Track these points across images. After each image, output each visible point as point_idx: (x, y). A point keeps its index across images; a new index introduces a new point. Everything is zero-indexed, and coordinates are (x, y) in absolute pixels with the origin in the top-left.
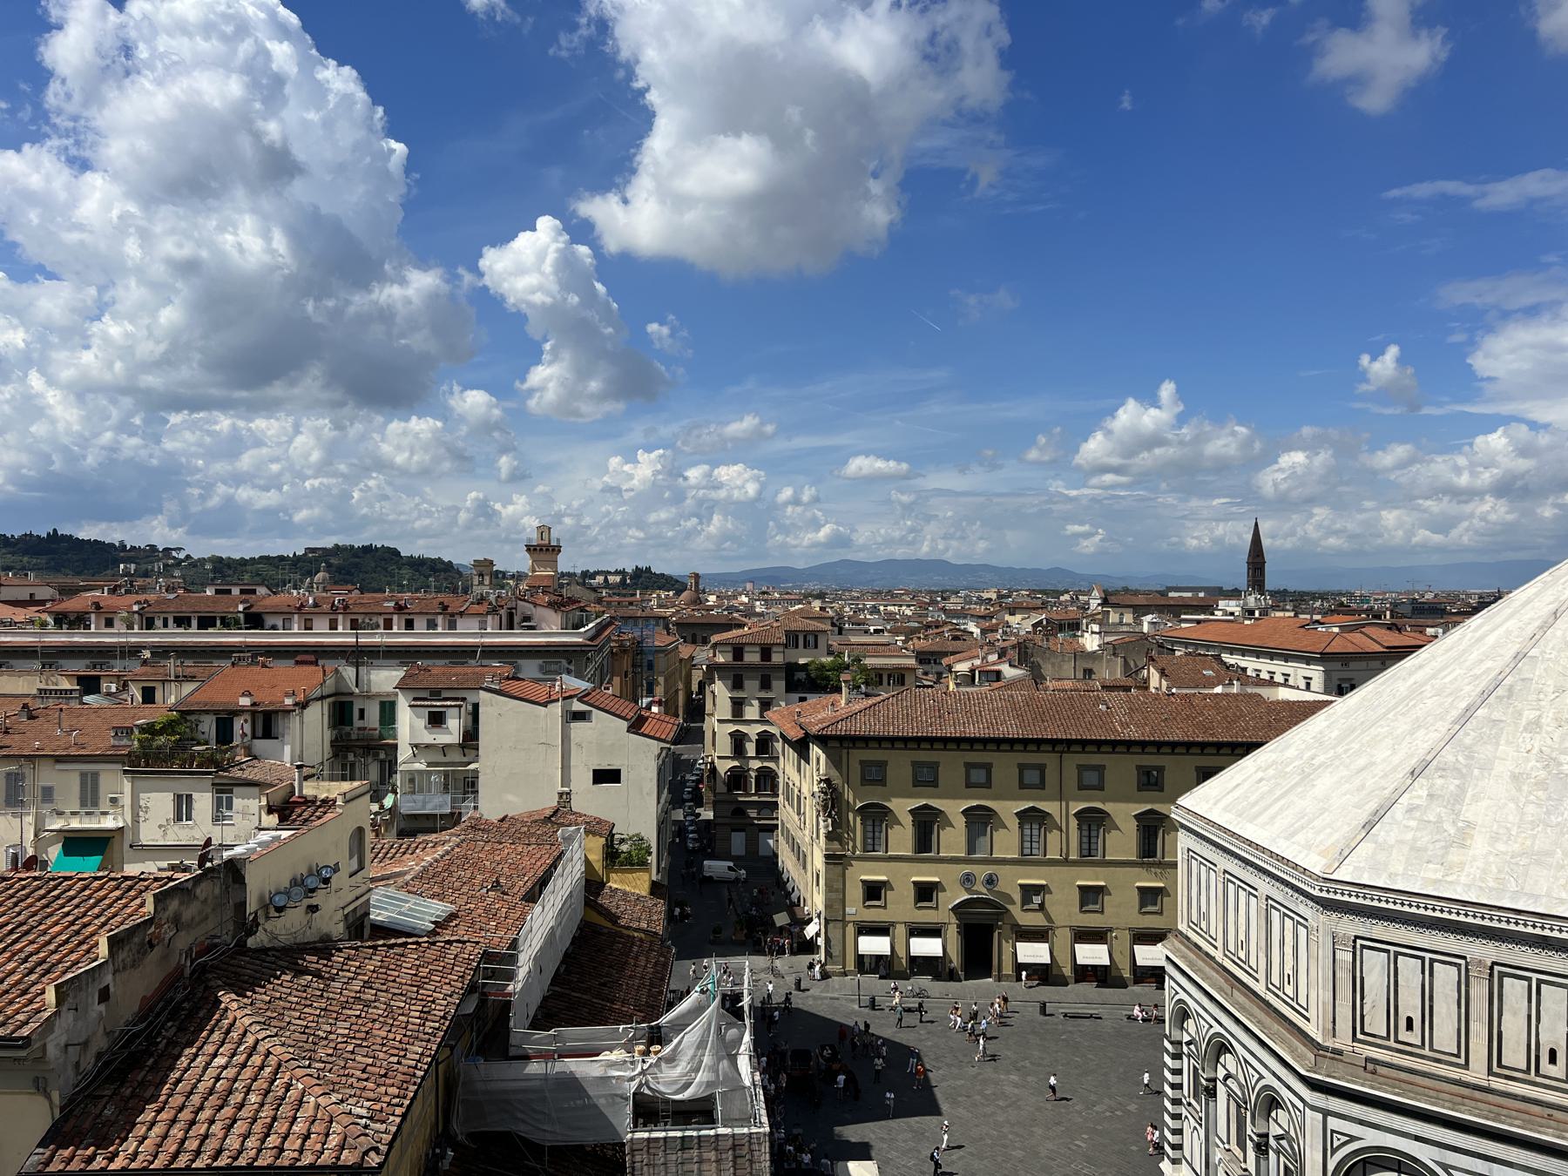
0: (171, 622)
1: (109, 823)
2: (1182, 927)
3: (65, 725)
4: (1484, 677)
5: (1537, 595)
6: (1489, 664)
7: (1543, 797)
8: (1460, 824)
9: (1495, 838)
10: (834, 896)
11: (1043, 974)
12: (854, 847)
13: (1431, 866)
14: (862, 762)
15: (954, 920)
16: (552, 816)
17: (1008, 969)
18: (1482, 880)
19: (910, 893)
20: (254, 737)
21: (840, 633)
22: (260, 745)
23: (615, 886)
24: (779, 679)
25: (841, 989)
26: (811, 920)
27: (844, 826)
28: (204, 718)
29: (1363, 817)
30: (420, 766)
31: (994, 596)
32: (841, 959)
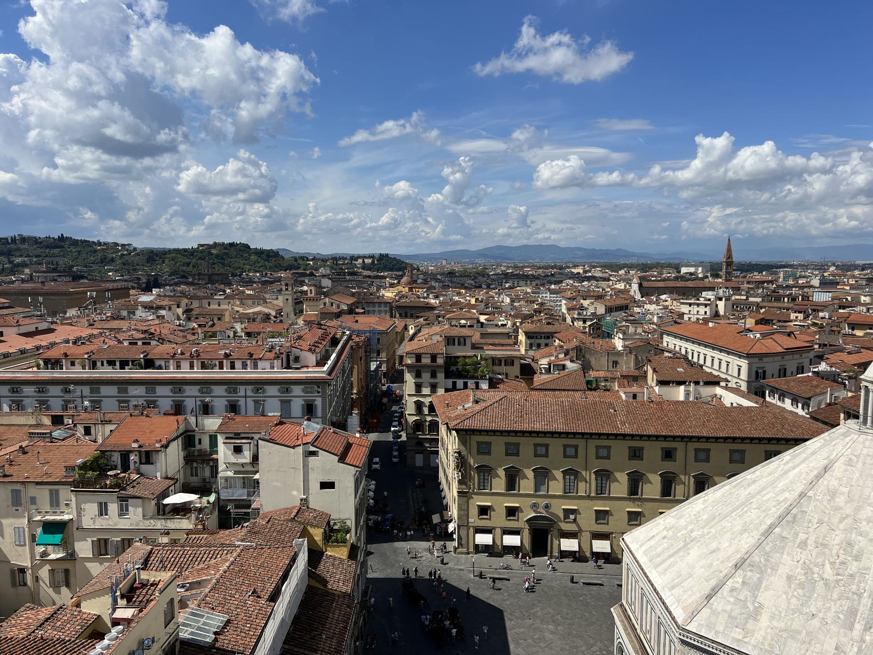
0: (105, 363)
1: (66, 517)
2: (624, 602)
3: (41, 458)
4: (783, 504)
5: (820, 448)
6: (786, 495)
7: (801, 594)
8: (756, 605)
9: (772, 618)
10: (462, 513)
11: (576, 557)
12: (474, 488)
13: (738, 630)
14: (478, 443)
15: (527, 527)
16: (295, 516)
18: (763, 644)
19: (504, 512)
20: (141, 463)
21: (482, 327)
22: (145, 468)
23: (330, 554)
25: (465, 563)
26: (451, 521)
27: (468, 477)
28: (113, 453)
29: (707, 591)
30: (230, 474)
31: (581, 271)
32: (466, 546)
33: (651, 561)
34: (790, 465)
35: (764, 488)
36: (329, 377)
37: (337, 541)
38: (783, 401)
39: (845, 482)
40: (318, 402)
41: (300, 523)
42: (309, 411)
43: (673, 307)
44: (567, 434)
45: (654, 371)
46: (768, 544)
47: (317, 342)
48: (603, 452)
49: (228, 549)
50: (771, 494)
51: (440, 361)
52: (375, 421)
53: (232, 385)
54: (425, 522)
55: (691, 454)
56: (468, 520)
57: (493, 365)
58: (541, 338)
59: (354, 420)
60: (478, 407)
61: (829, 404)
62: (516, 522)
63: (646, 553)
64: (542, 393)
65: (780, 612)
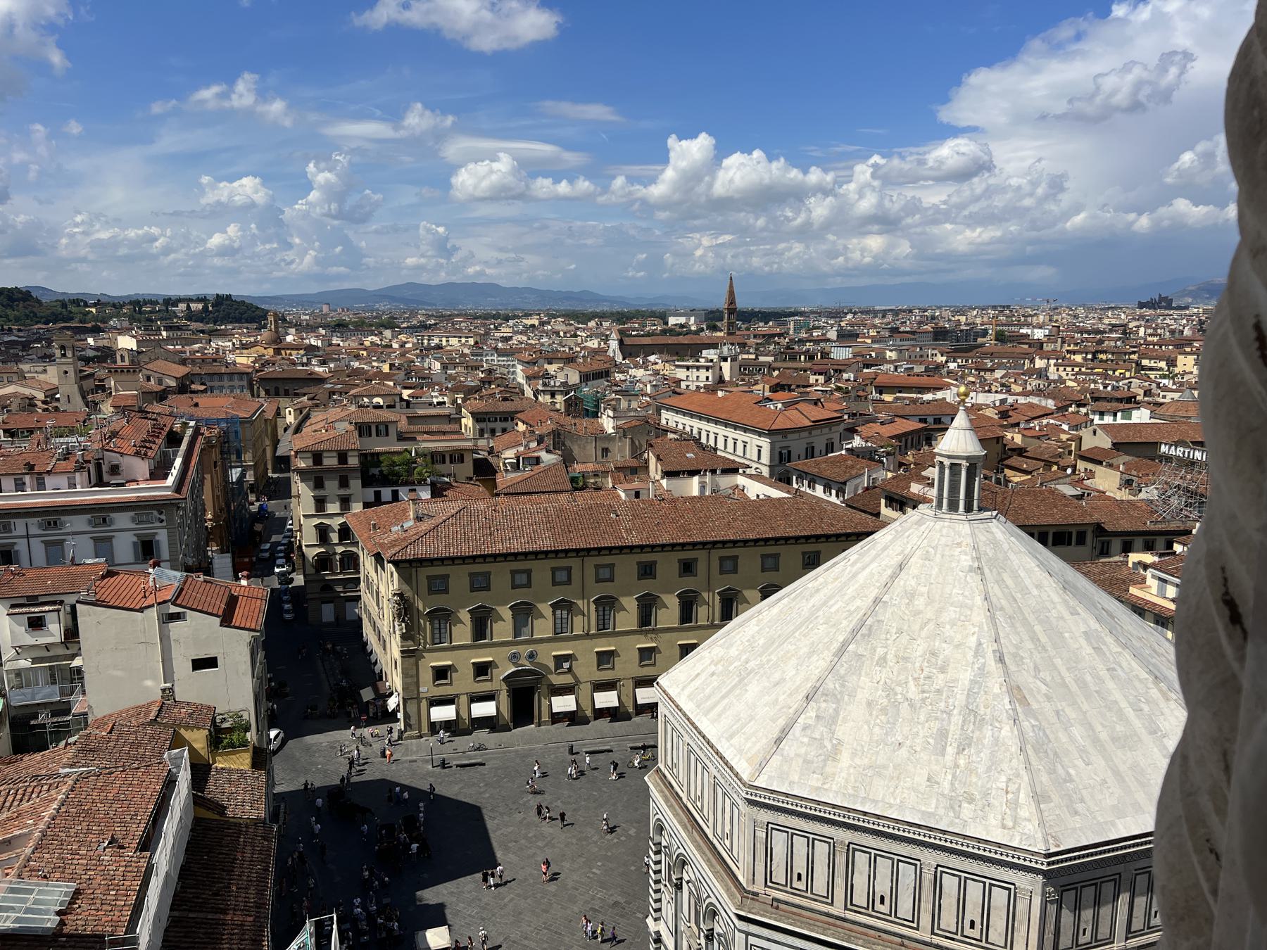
2: (661, 766)
5: (892, 541)
6: (858, 603)
8: (834, 742)
9: (854, 755)
10: (409, 680)
11: (572, 718)
12: (425, 643)
13: (815, 776)
14: (428, 577)
15: (505, 687)
16: (157, 717)
17: (546, 717)
18: (846, 788)
19: (470, 671)
21: (408, 407)
23: (221, 766)
24: (356, 478)
25: (417, 751)
26: (391, 694)
27: (416, 628)
29: (775, 734)
30: (25, 663)
31: (537, 323)
32: (417, 726)
33: (698, 706)
34: (859, 565)
35: (831, 598)
36: (178, 496)
37: (232, 745)
39: (923, 580)
40: (162, 537)
41: (166, 725)
42: (147, 550)
44: (556, 552)
45: (658, 458)
46: (842, 666)
47: (145, 441)
48: (605, 573)
49: (49, 782)
50: (840, 604)
51: (353, 461)
54: (350, 701)
55: (715, 564)
56: (418, 690)
57: (433, 463)
59: (222, 562)
60: (424, 527)
61: (867, 489)
62: (489, 684)
63: (691, 698)
64: (513, 499)
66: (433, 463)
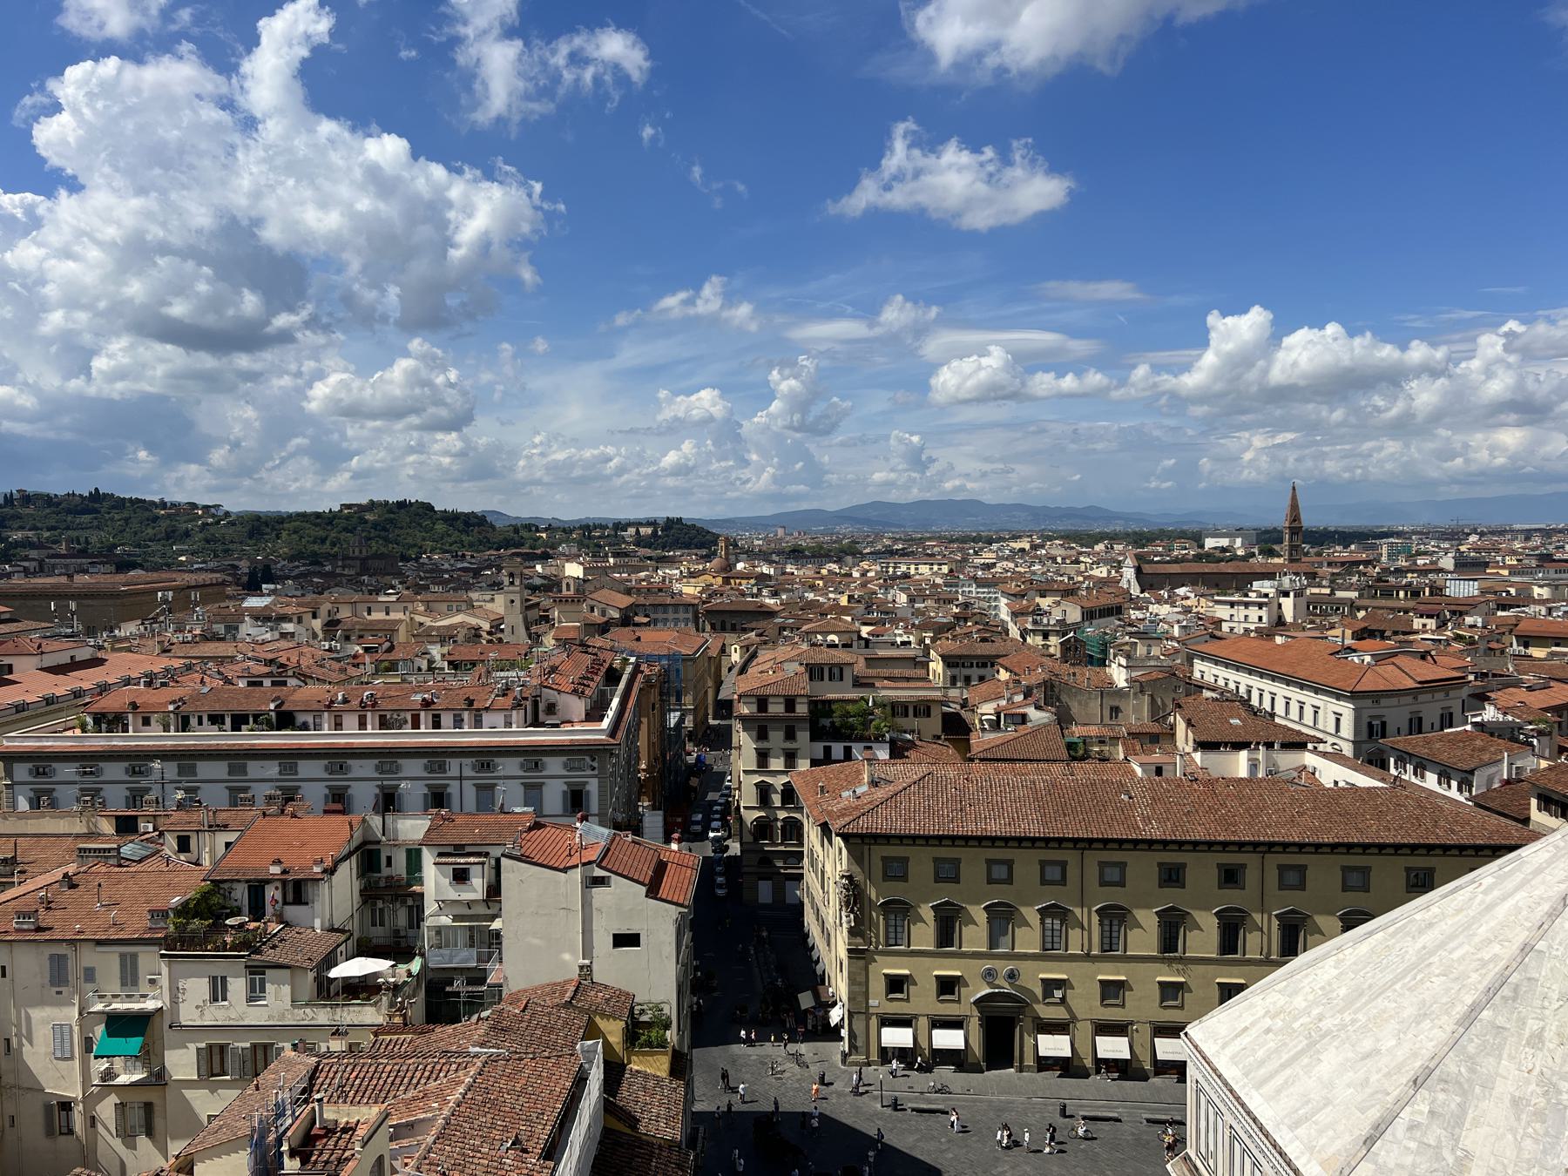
0: (205, 719)
1: (150, 1005)
2: (1191, 1152)
3: (104, 895)
4: (1491, 966)
5: (1550, 862)
6: (1496, 949)
7: (1541, 1132)
8: (1459, 1153)
10: (856, 988)
11: (1066, 1067)
12: (878, 943)
14: (884, 859)
15: (976, 1013)
16: (572, 998)
17: (1029, 1061)
19: (933, 987)
20: (285, 903)
21: (867, 646)
22: (292, 912)
23: (636, 1068)
24: (804, 730)
26: (834, 1004)
27: (867, 923)
28: (235, 885)
29: (1365, 1130)
30: (446, 920)
31: (1027, 546)
33: (1246, 1075)
34: (1496, 893)
35: (1452, 937)
36: (612, 741)
37: (649, 1044)
38: (1423, 777)
40: (593, 786)
41: (581, 1010)
42: (576, 801)
43: (1199, 609)
44: (1047, 840)
45: (1189, 723)
46: (1472, 1041)
47: (584, 678)
48: (1111, 873)
49: (458, 1060)
50: (1466, 948)
51: (802, 709)
52: (679, 820)
53: (436, 756)
54: (785, 1006)
56: (867, 1003)
57: (893, 715)
58: (972, 666)
59: (653, 821)
60: (880, 794)
61: (1508, 782)
62: (956, 1005)
63: (1234, 1059)
64: (990, 767)
65: (1505, 1167)
66: (893, 715)
